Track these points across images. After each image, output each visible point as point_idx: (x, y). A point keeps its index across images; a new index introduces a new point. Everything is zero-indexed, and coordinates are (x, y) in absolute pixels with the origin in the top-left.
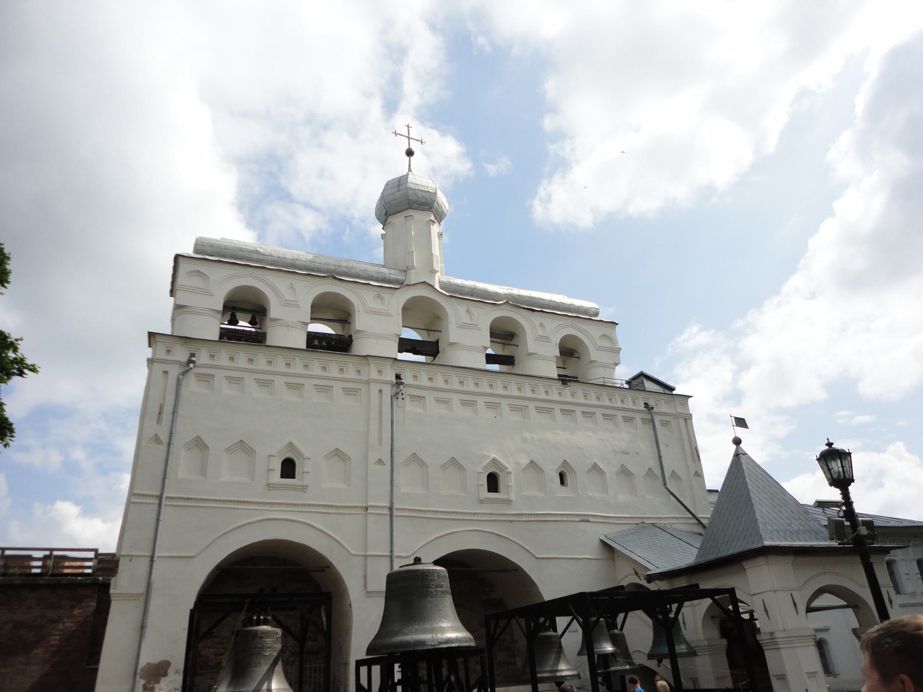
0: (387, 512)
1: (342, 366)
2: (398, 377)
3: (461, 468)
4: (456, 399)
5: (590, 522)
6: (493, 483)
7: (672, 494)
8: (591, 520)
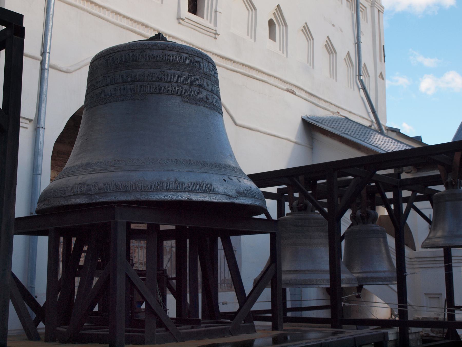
5: (295, 94)
7: (364, 89)
8: (297, 93)
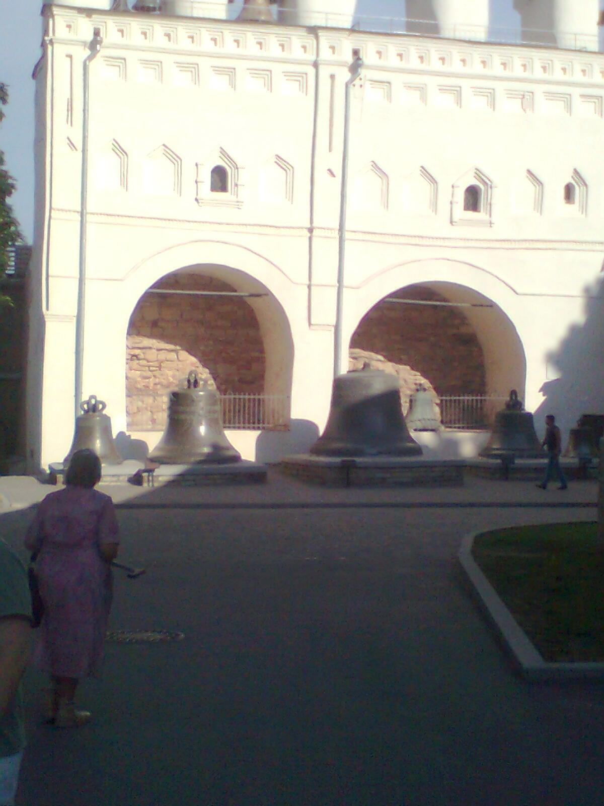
0: (336, 234)
1: (283, 41)
2: (356, 53)
3: (433, 180)
4: (432, 83)
6: (473, 198)
